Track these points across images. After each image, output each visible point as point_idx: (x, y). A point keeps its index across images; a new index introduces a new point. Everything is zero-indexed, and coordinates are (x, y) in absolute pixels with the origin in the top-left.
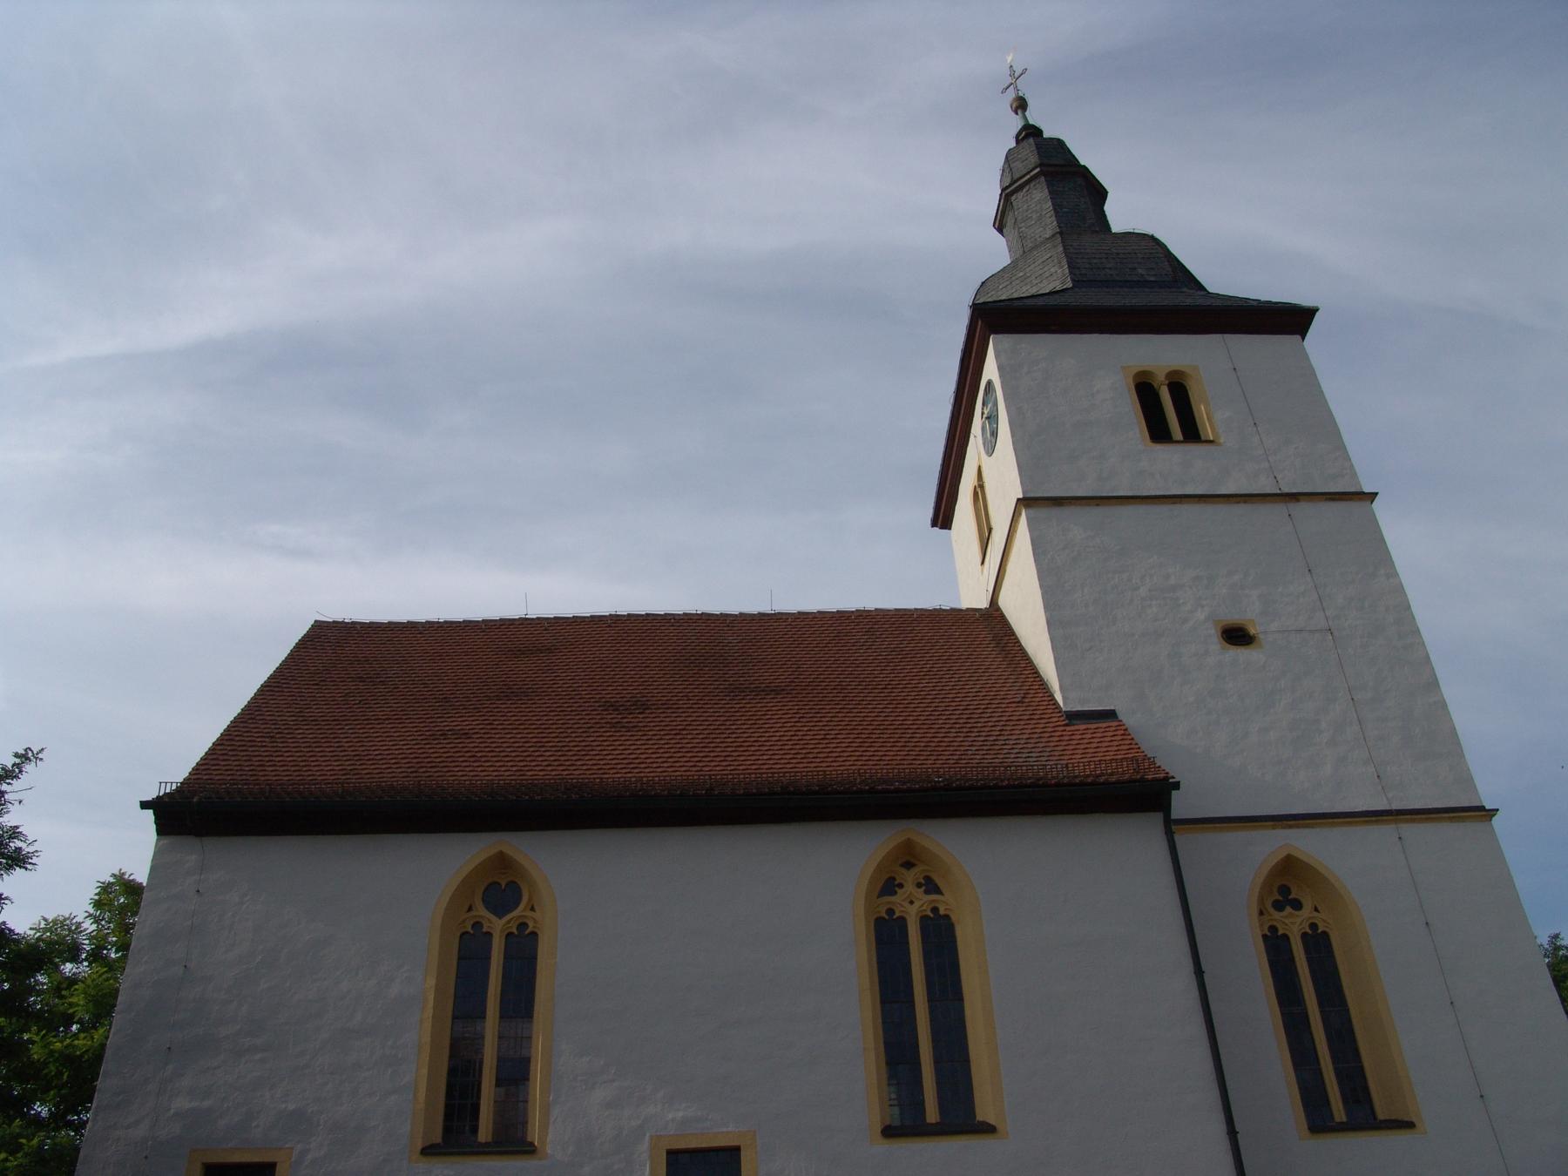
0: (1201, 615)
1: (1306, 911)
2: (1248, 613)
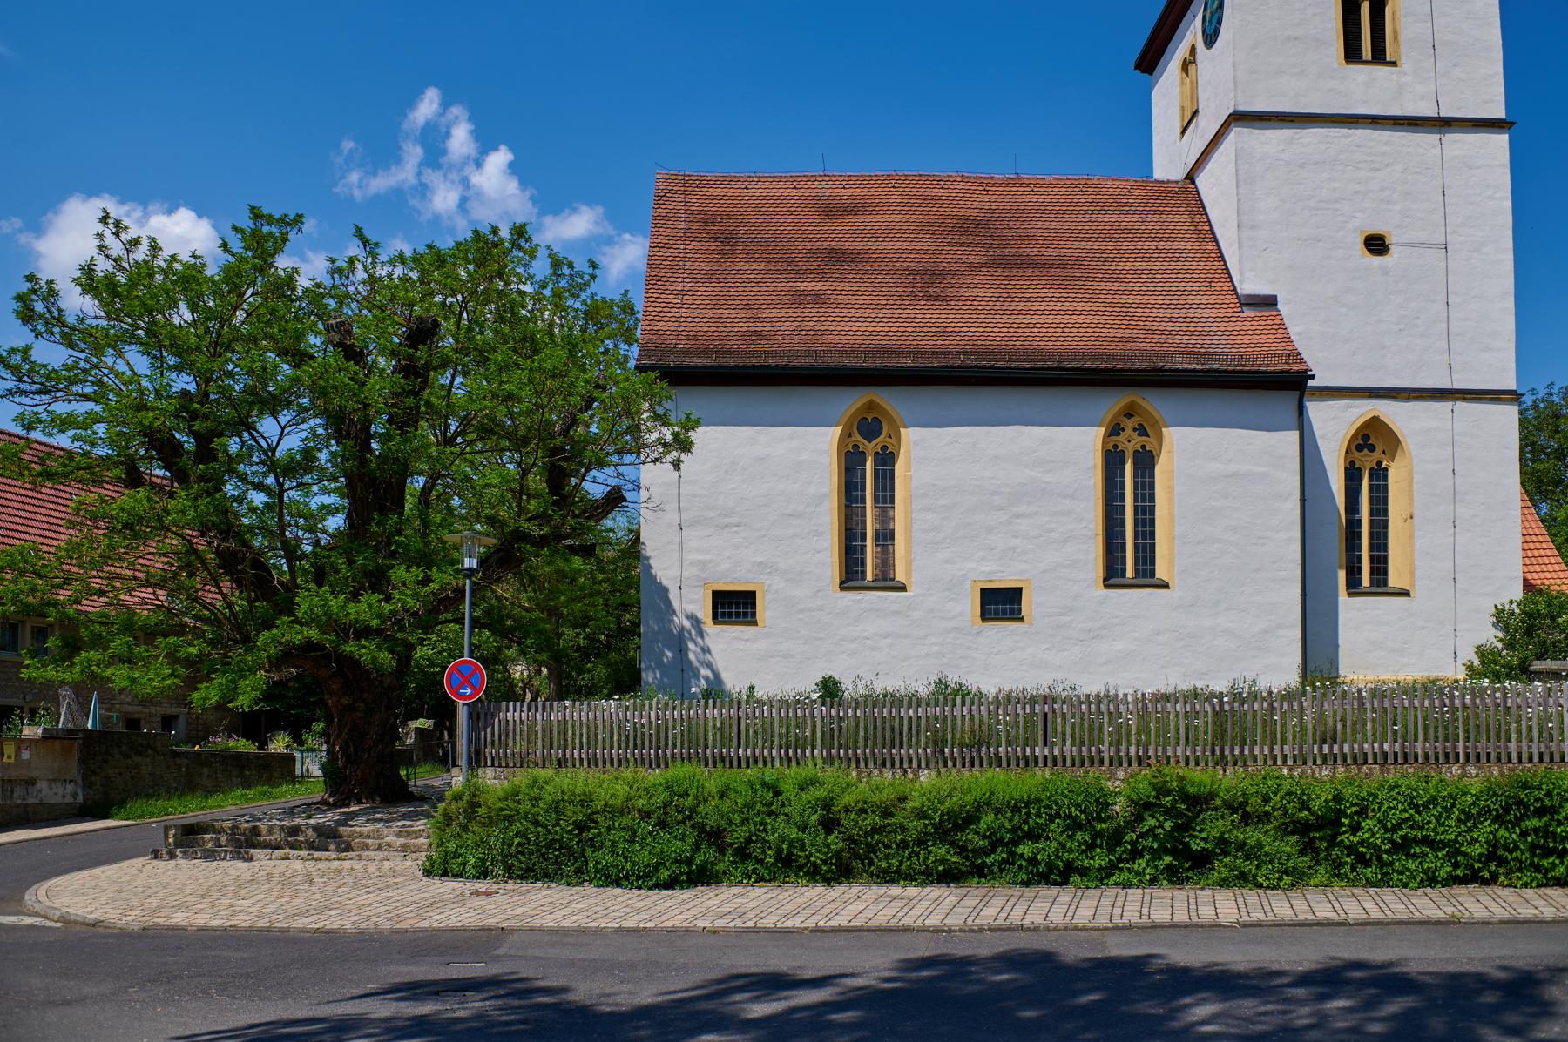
1: (1377, 455)
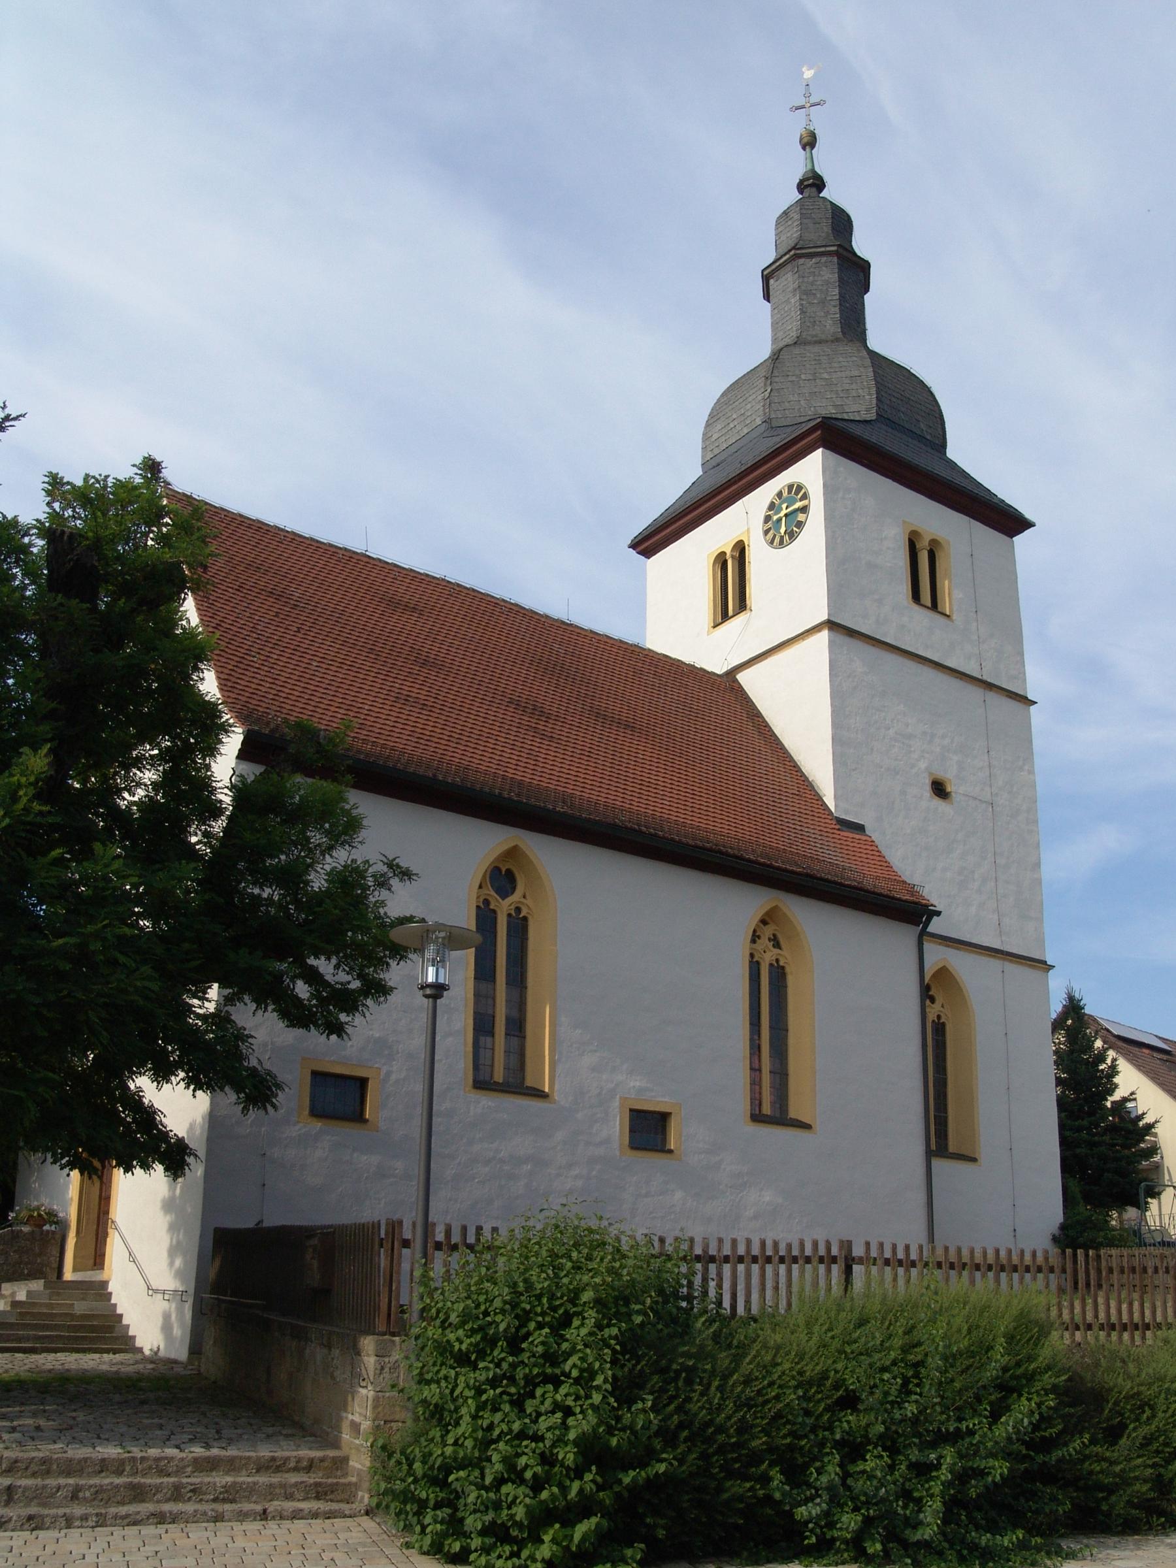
0: (923, 765)
2: (949, 775)
